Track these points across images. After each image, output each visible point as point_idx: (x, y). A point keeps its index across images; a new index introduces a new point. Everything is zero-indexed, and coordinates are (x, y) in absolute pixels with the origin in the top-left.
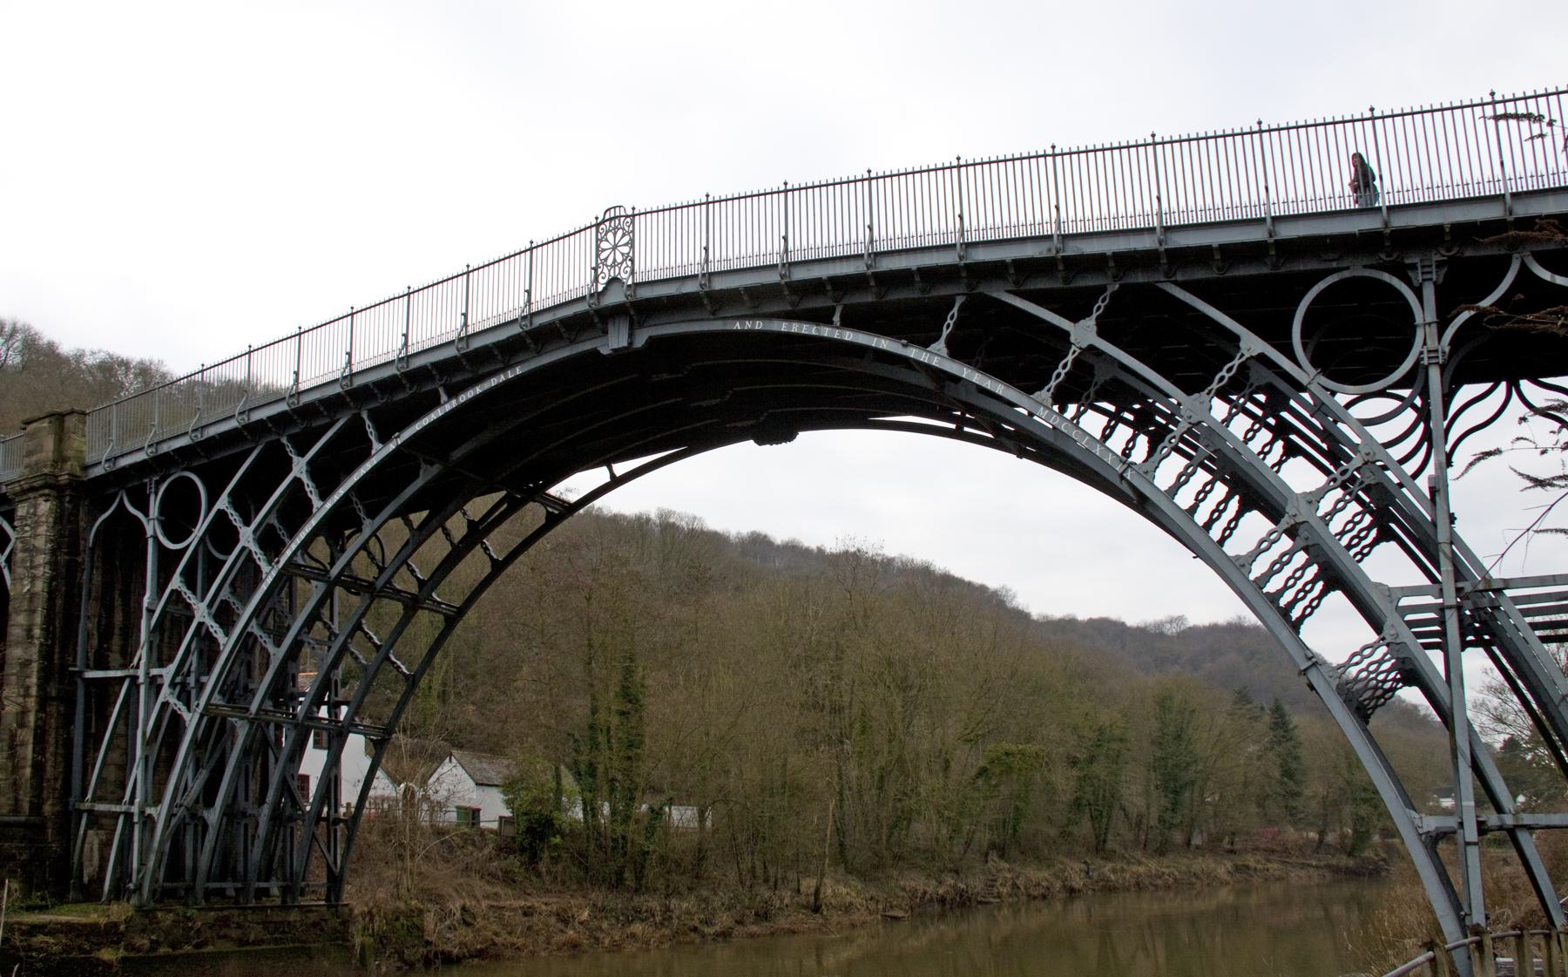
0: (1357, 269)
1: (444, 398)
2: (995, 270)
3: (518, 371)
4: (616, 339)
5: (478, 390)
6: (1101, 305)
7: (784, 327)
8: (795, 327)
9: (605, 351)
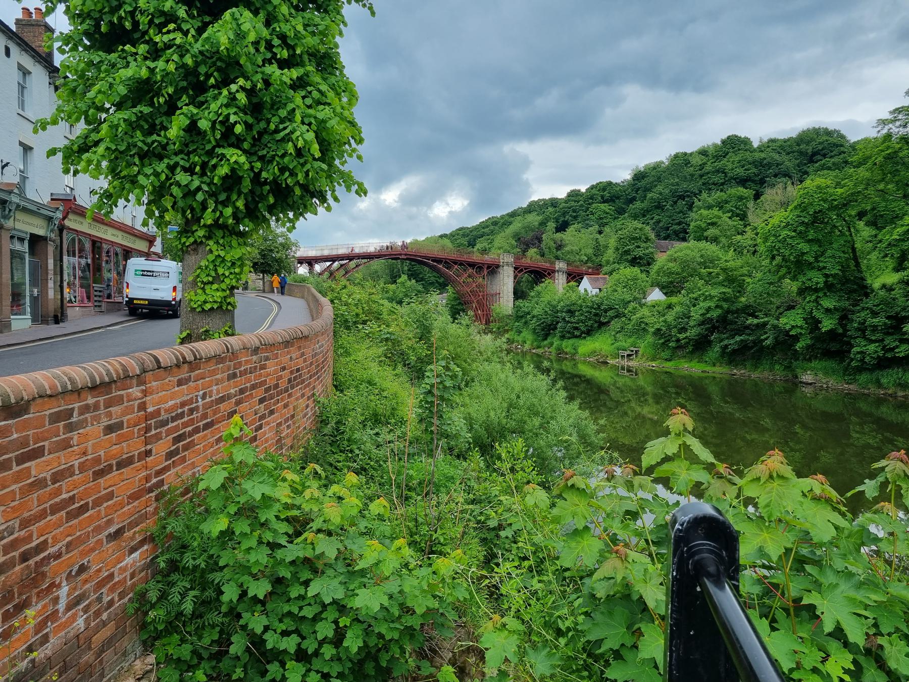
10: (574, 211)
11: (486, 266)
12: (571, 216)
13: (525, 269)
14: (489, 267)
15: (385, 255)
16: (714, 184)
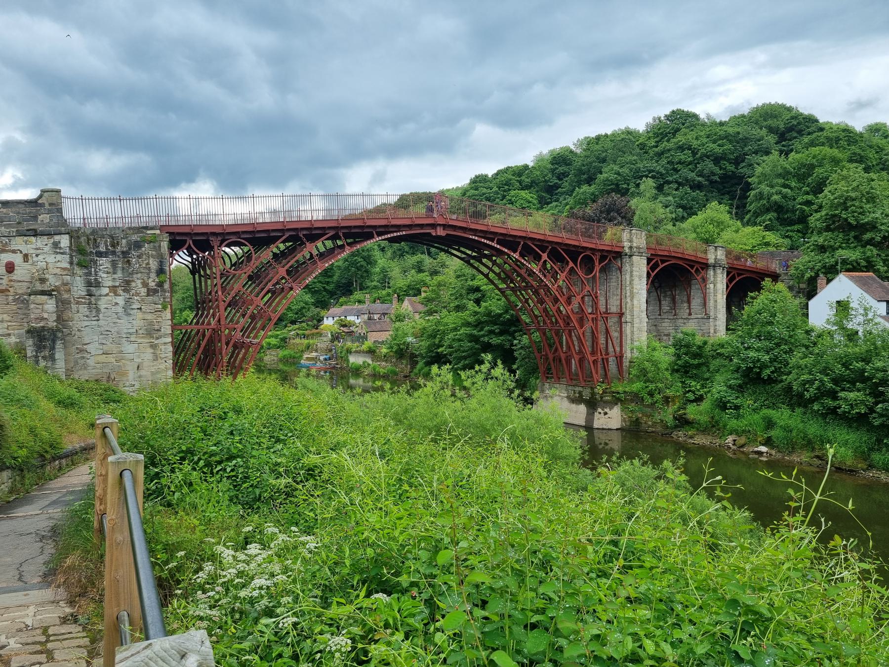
0: (588, 253)
1: (375, 236)
2: (531, 239)
3: (404, 233)
4: (441, 232)
5: (389, 236)
6: (548, 251)
7: (483, 240)
8: (485, 241)
9: (434, 234)
10: (488, 199)
11: (598, 254)
12: (485, 205)
13: (663, 262)
14: (603, 258)
15: (398, 228)
16: (680, 163)
